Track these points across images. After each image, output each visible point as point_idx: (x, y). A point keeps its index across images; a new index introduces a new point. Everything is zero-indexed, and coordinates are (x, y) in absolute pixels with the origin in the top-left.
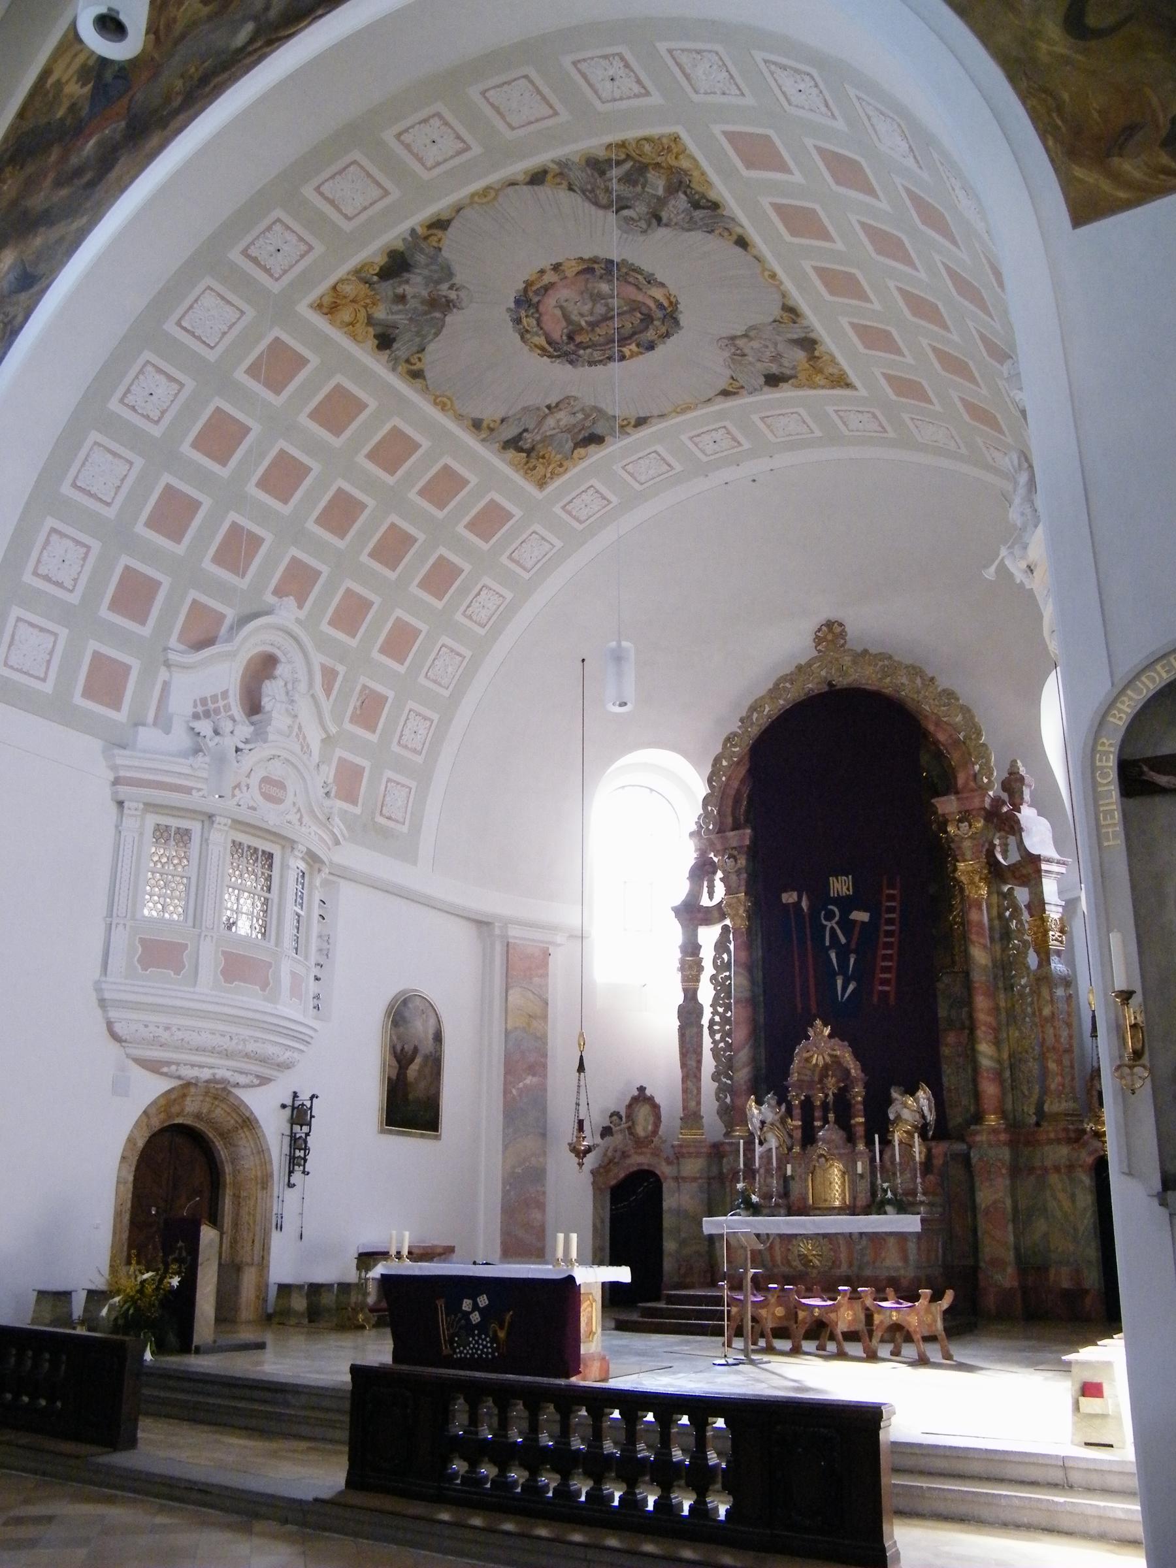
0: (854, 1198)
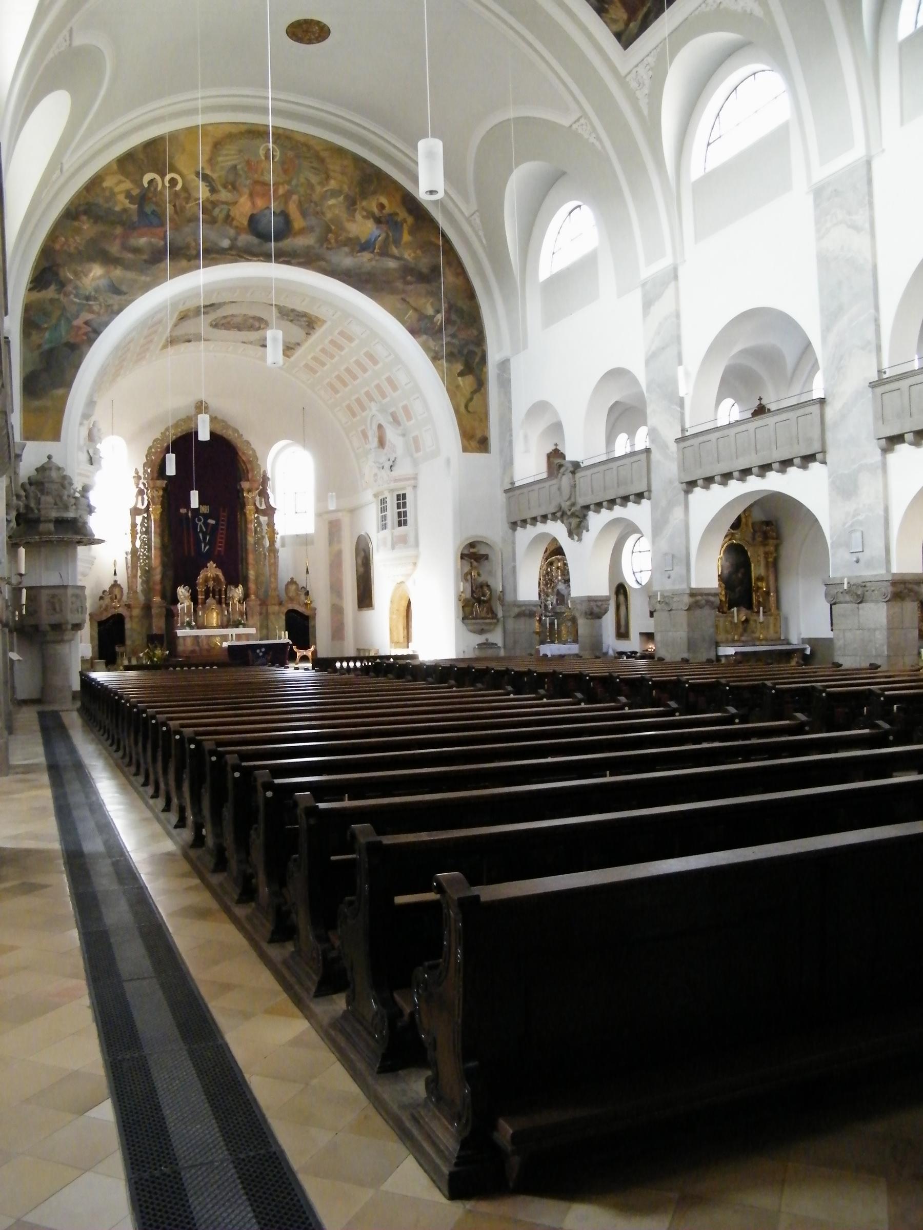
0: (222, 623)
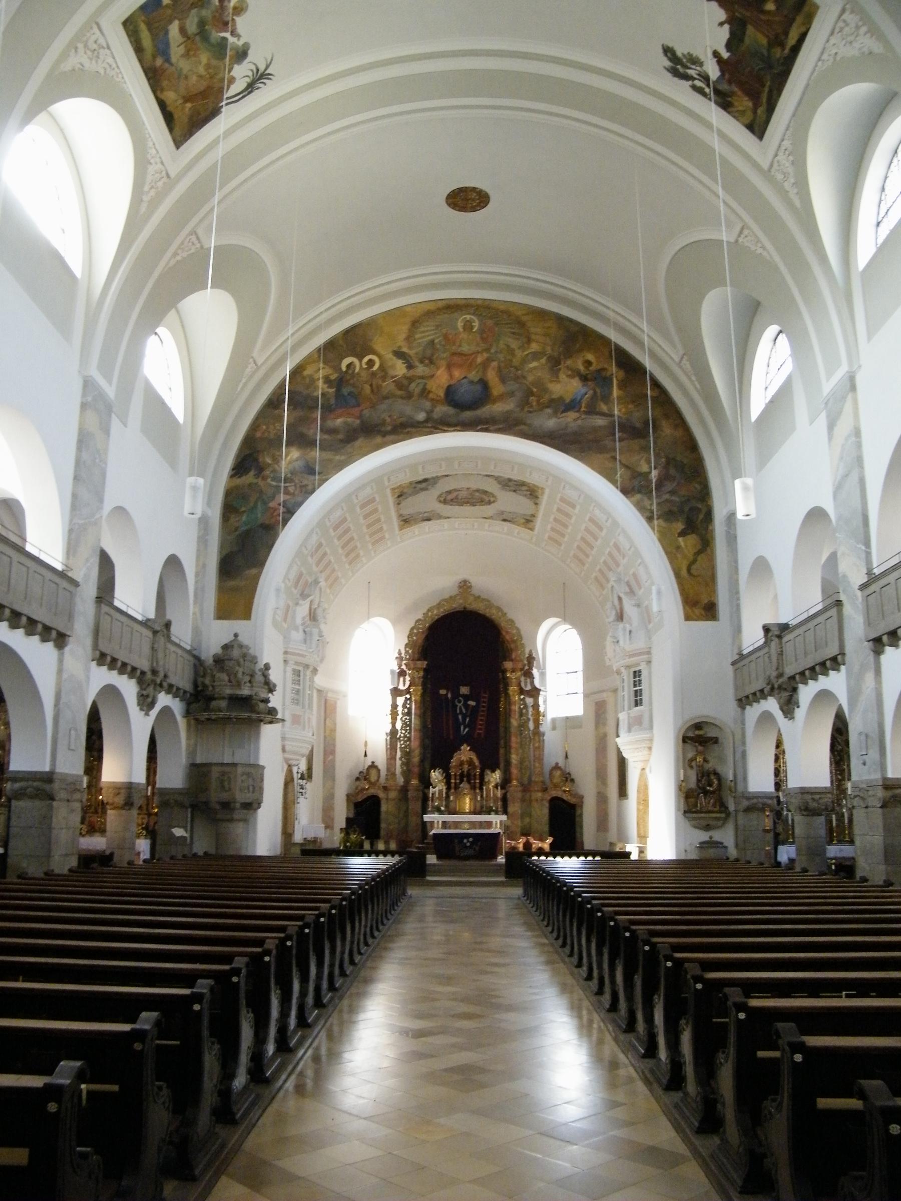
0: (475, 809)
